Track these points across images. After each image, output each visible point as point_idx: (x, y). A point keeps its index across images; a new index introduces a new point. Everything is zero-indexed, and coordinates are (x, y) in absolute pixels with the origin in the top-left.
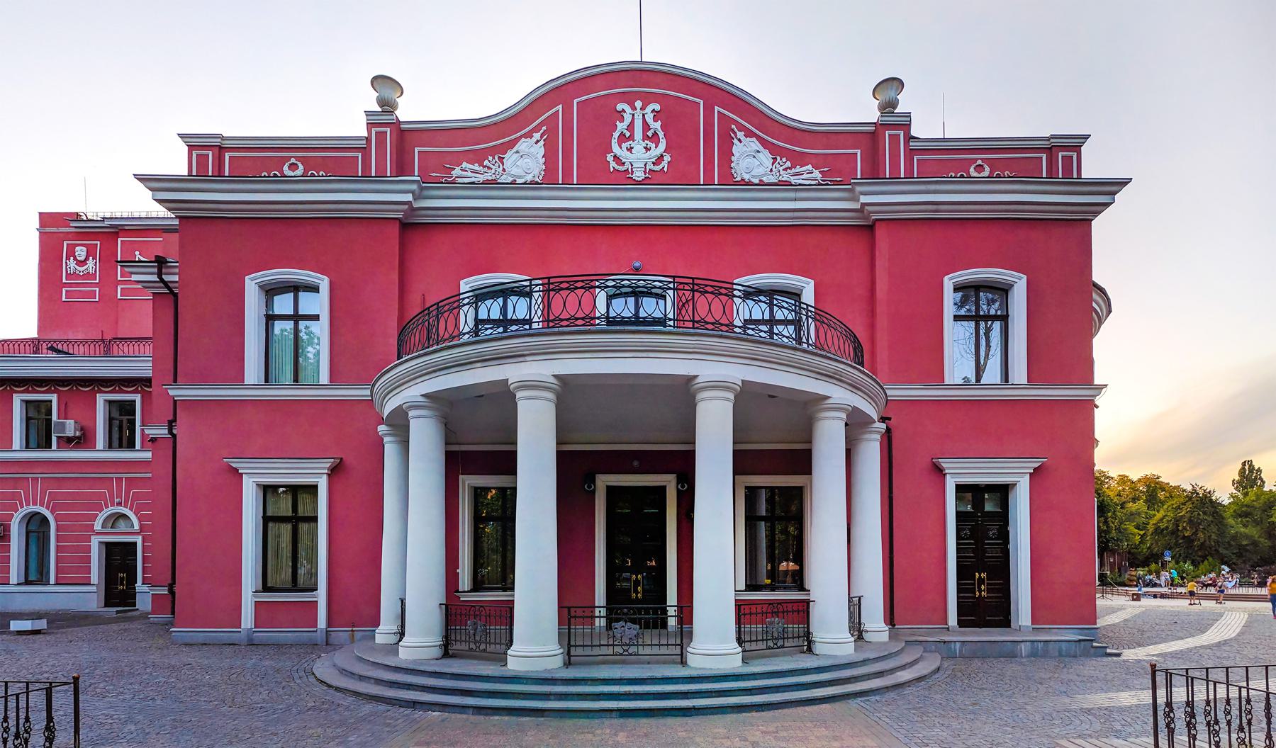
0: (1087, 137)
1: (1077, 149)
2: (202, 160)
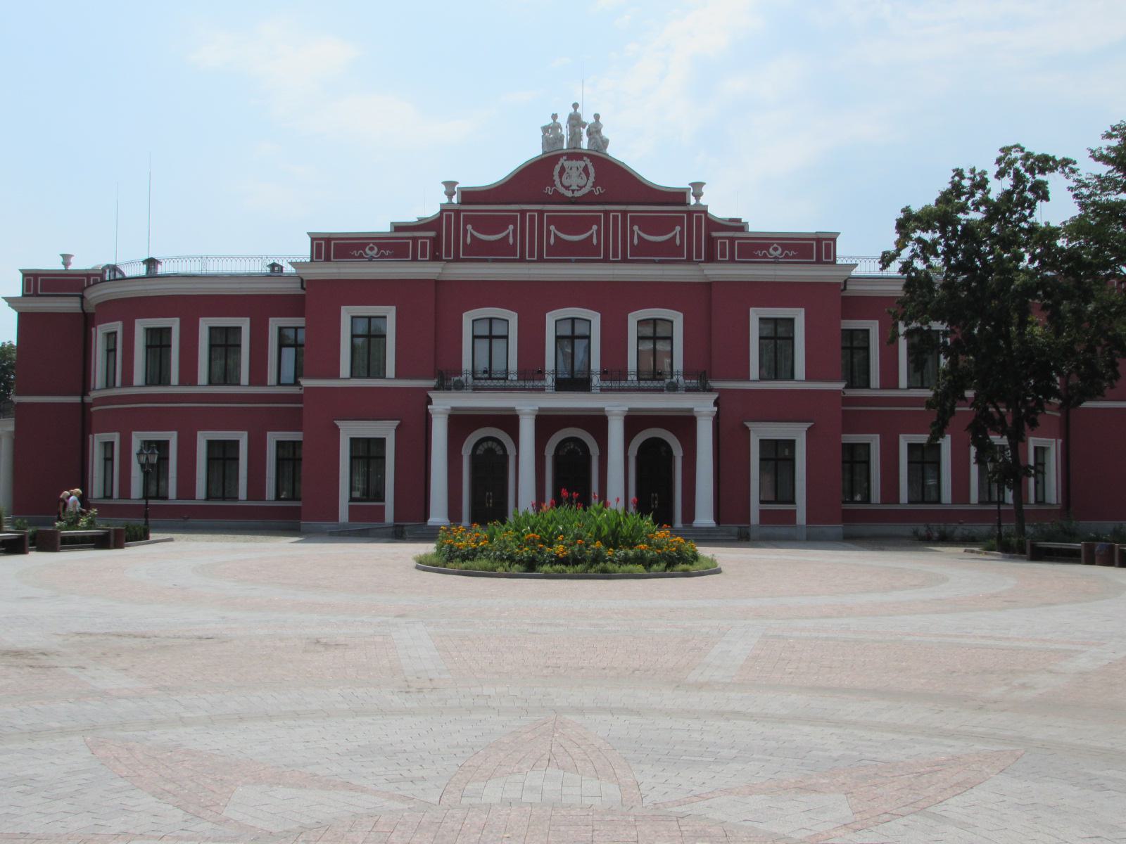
0: (838, 234)
1: (834, 240)
2: (319, 246)
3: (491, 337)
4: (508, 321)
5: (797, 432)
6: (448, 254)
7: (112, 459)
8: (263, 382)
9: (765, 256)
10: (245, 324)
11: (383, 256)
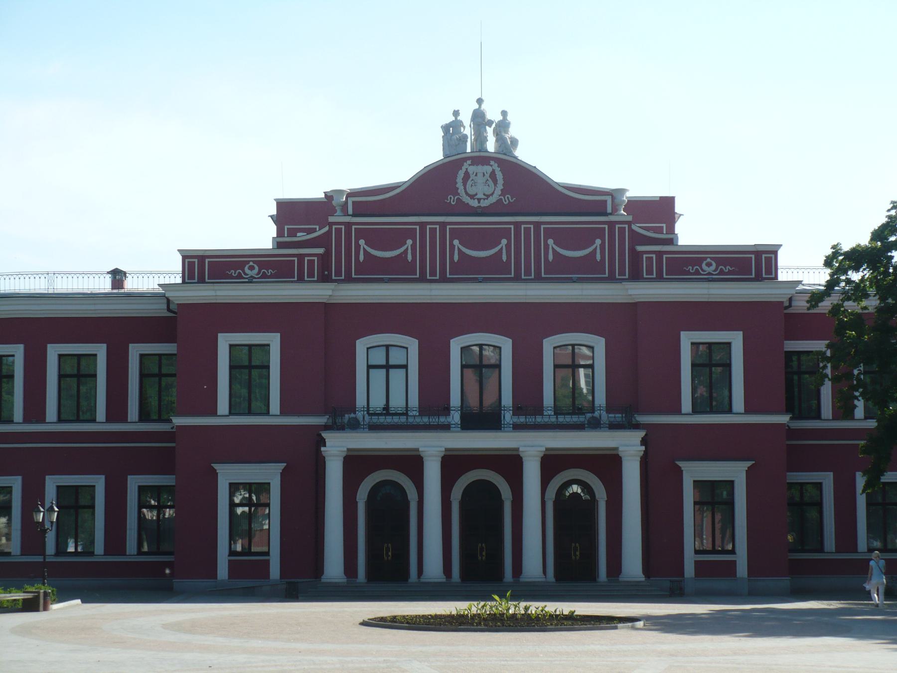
1: (775, 253)
2: (191, 265)
3: (388, 367)
4: (407, 348)
5: (736, 472)
6: (338, 273)
8: (123, 419)
9: (697, 273)
10: (100, 351)
11: (264, 276)
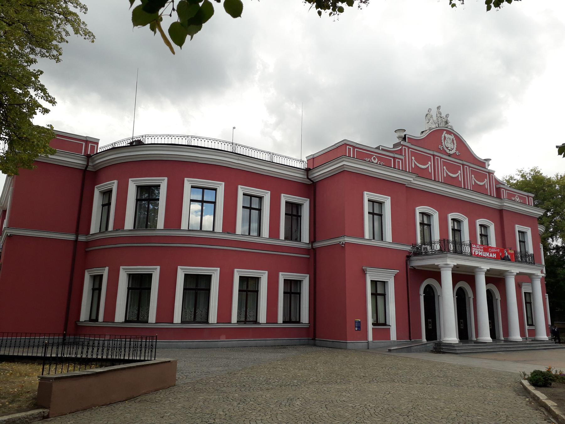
7: (100, 289)
